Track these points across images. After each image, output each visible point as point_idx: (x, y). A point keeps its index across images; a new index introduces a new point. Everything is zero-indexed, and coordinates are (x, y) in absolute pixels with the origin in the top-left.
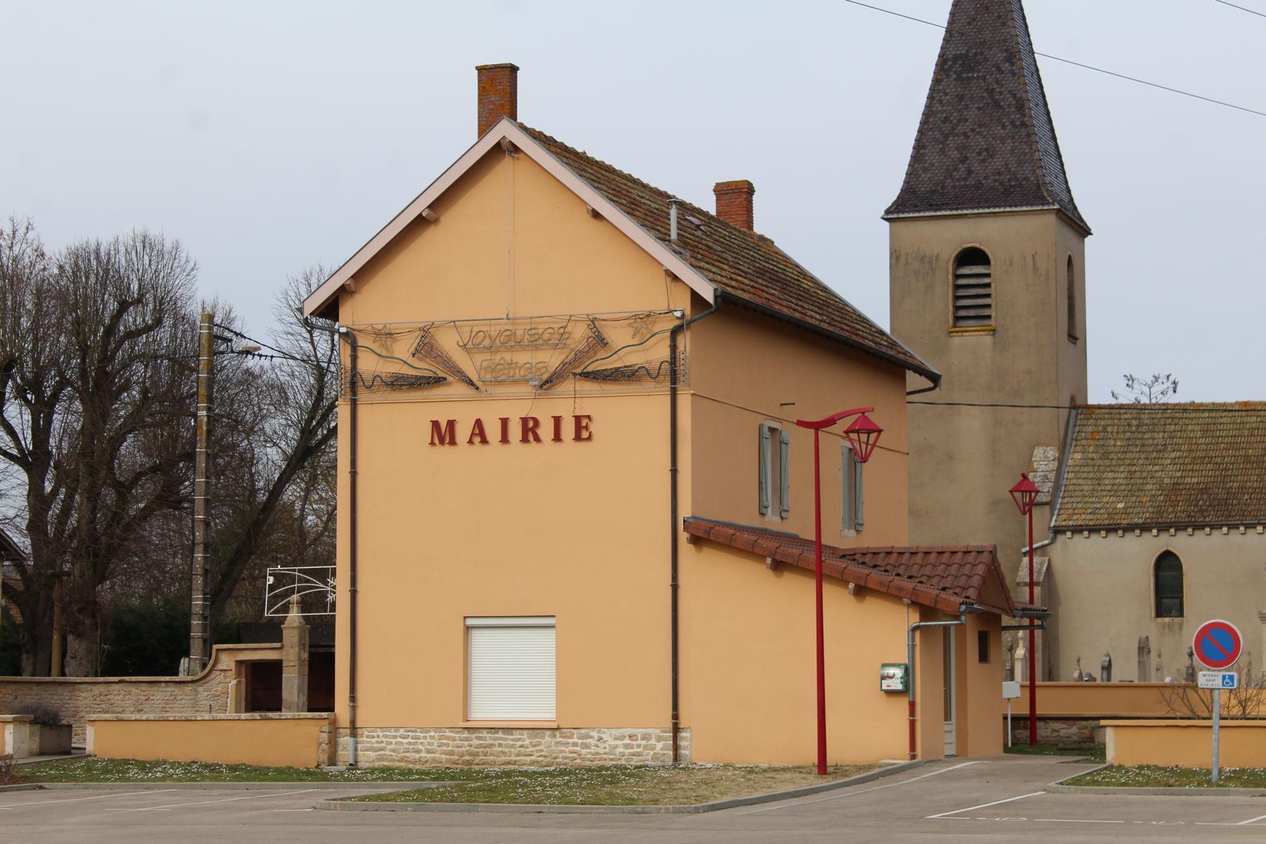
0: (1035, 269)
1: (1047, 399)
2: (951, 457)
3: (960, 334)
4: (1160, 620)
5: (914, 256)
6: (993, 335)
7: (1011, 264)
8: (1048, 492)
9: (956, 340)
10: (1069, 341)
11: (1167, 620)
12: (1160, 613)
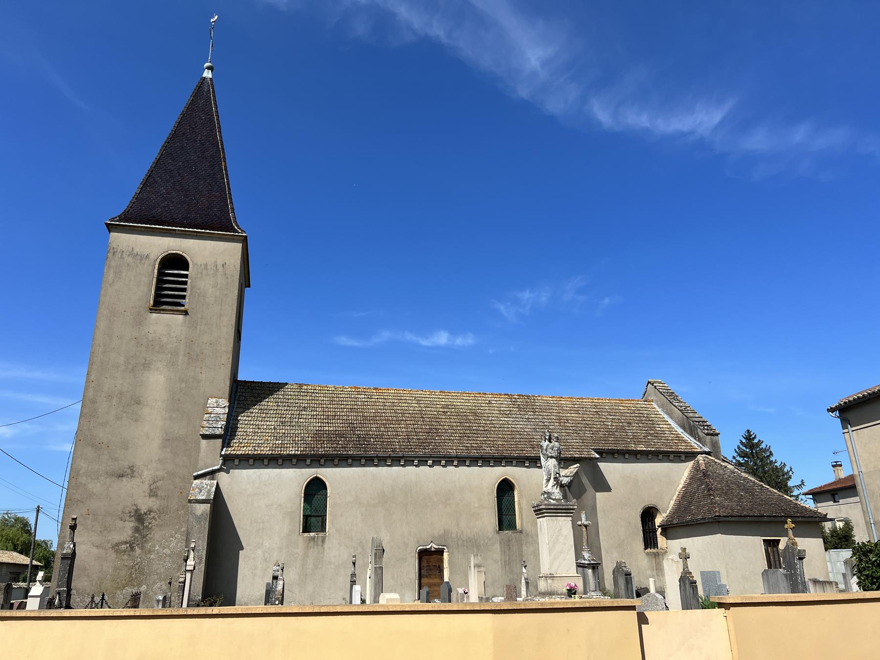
1: (223, 364)
2: (138, 403)
4: (306, 534)
5: (128, 253)
8: (221, 428)
9: (154, 315)
11: (312, 534)
12: (306, 530)
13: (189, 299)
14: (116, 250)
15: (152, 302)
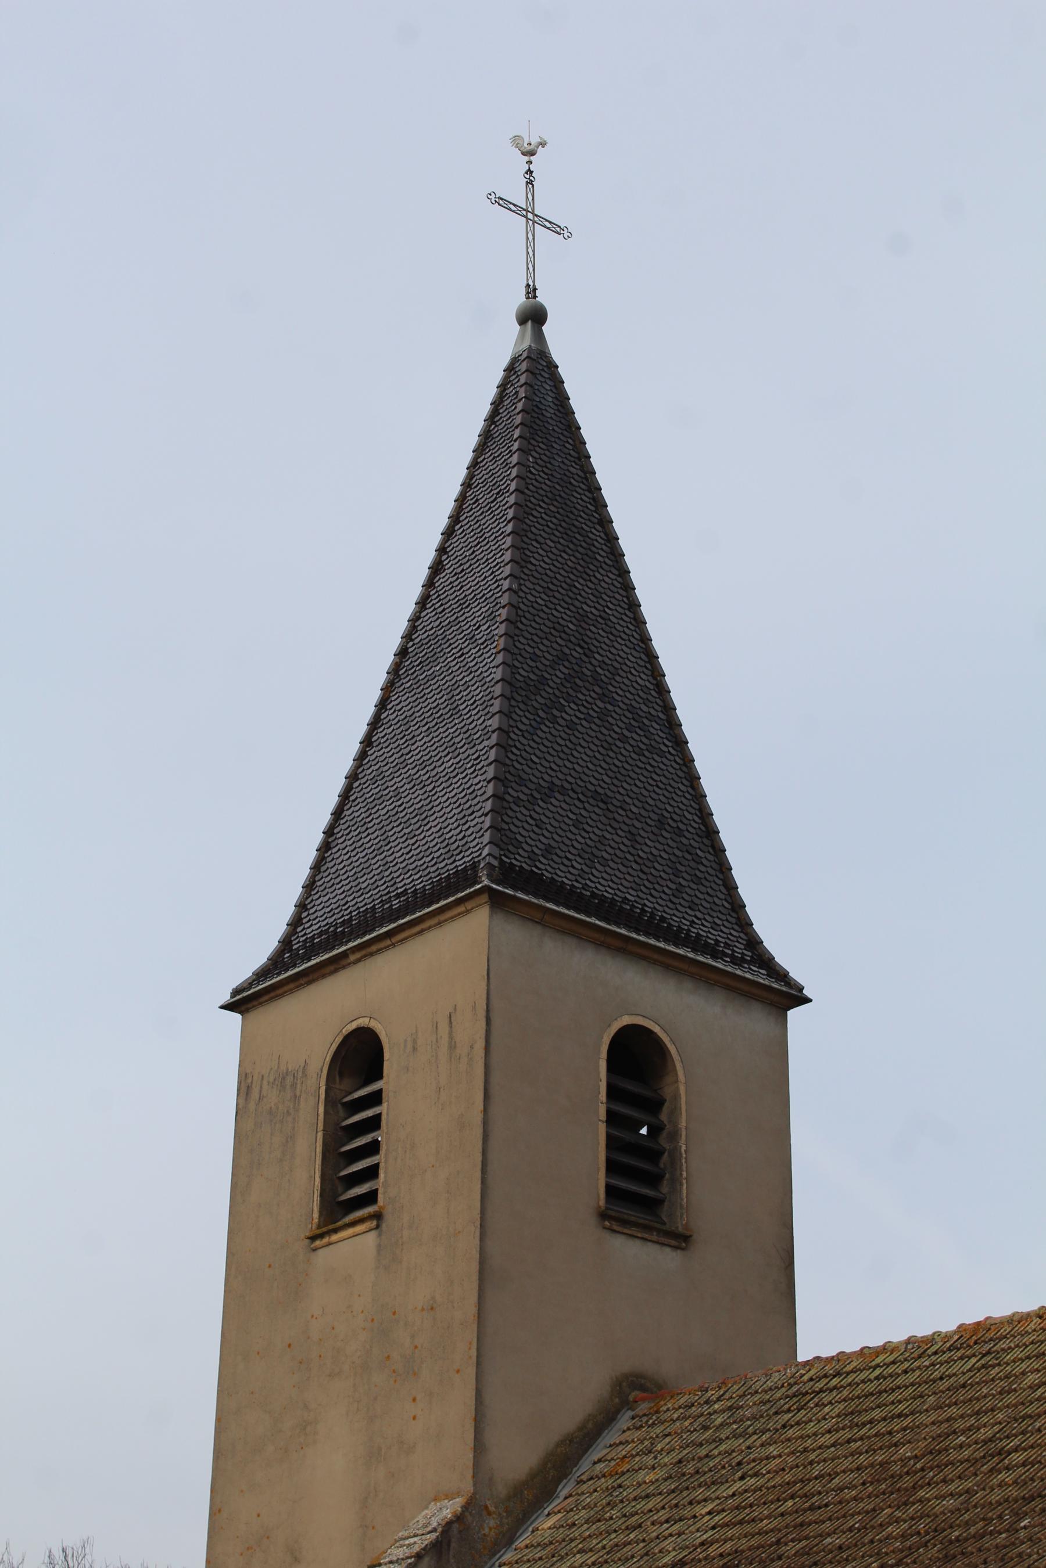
0: (452, 1046)
1: (458, 1371)
2: (297, 1560)
3: (326, 1240)
6: (378, 1227)
7: (415, 1049)
10: (604, 1228)
13: (385, 1172)
14: (249, 1081)
15: (316, 1215)
